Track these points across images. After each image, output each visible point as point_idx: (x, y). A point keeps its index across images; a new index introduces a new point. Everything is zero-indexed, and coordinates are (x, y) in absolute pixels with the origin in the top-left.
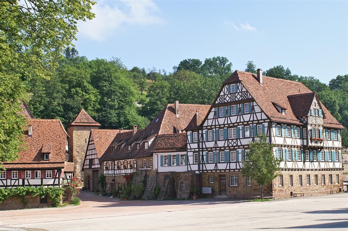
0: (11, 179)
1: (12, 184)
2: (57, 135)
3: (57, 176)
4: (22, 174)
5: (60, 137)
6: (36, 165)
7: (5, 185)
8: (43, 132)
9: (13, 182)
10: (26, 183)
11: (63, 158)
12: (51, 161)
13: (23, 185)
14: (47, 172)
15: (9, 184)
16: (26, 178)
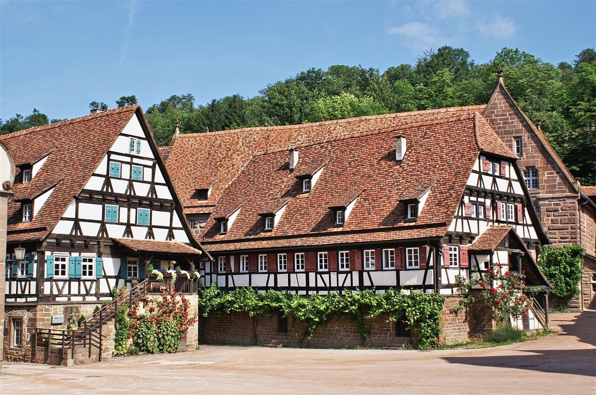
0: (339, 273)
1: (340, 285)
2: (458, 153)
3: (431, 264)
4: (356, 258)
5: (463, 156)
6: (384, 233)
7: (328, 285)
8: (429, 150)
9: (342, 277)
10: (367, 283)
11: (449, 213)
12: (419, 223)
13: (362, 287)
14: (410, 251)
15: (334, 284)
16: (365, 269)
